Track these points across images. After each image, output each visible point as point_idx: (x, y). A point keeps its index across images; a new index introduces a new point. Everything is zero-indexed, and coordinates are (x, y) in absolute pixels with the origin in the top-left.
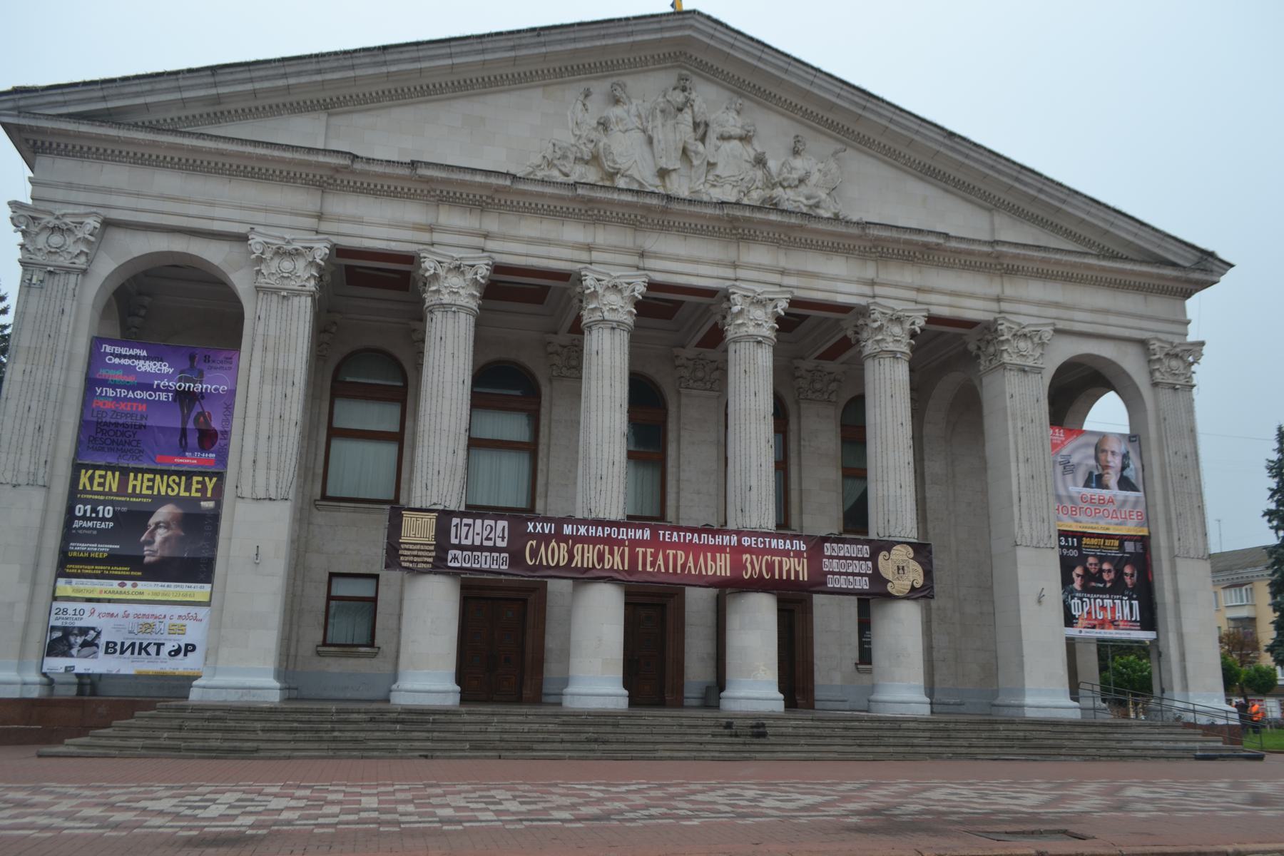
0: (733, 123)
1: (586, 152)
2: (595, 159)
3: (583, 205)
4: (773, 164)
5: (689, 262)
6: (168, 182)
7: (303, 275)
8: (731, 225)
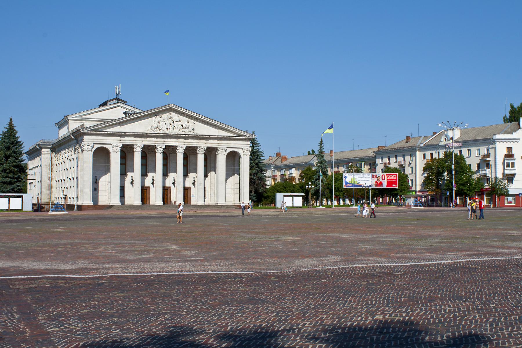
0: (178, 119)
1: (156, 127)
2: (157, 127)
3: (157, 136)
5: (171, 142)
8: (178, 137)
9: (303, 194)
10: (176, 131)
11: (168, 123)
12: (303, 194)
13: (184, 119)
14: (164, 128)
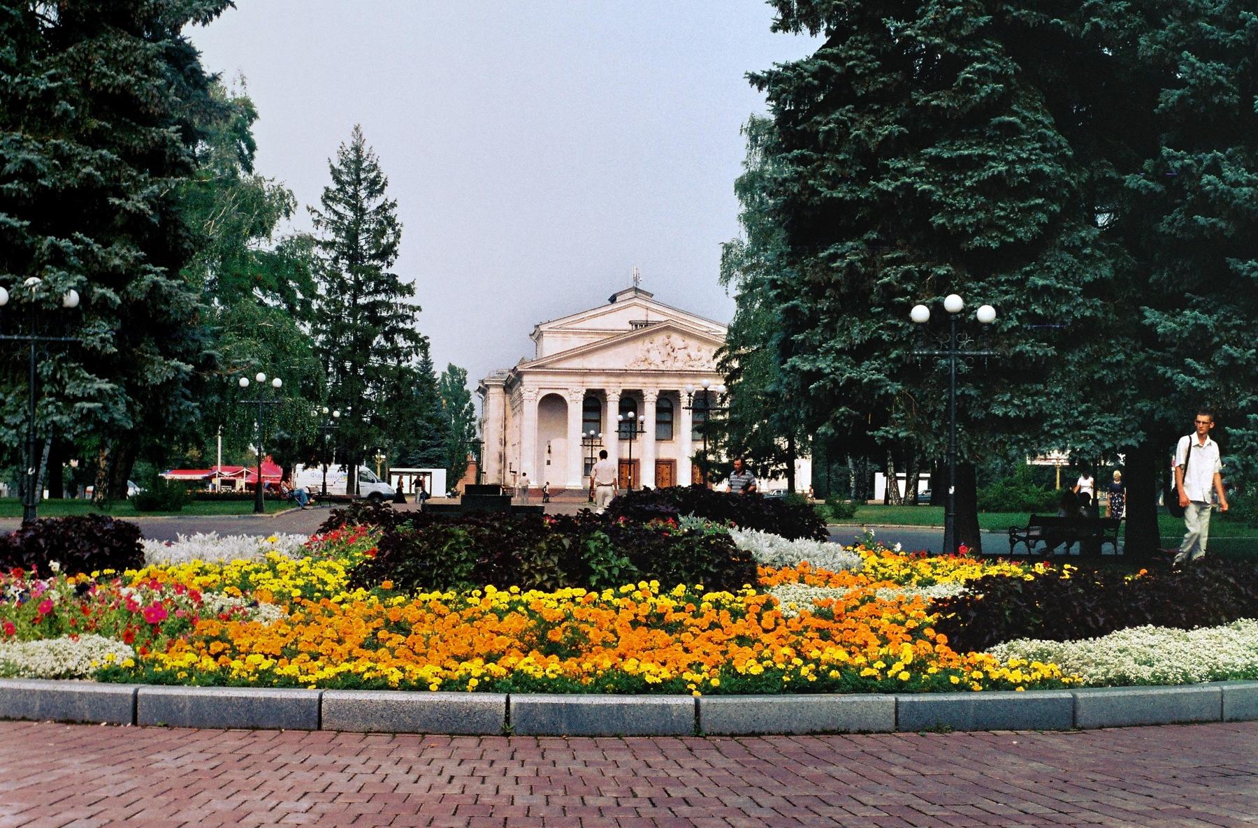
0: (682, 345)
4: (693, 355)
5: (670, 384)
6: (550, 378)
7: (581, 398)
8: (680, 374)
9: (928, 475)
10: (678, 366)
11: (664, 351)
12: (928, 475)
13: (693, 343)
14: (657, 360)
